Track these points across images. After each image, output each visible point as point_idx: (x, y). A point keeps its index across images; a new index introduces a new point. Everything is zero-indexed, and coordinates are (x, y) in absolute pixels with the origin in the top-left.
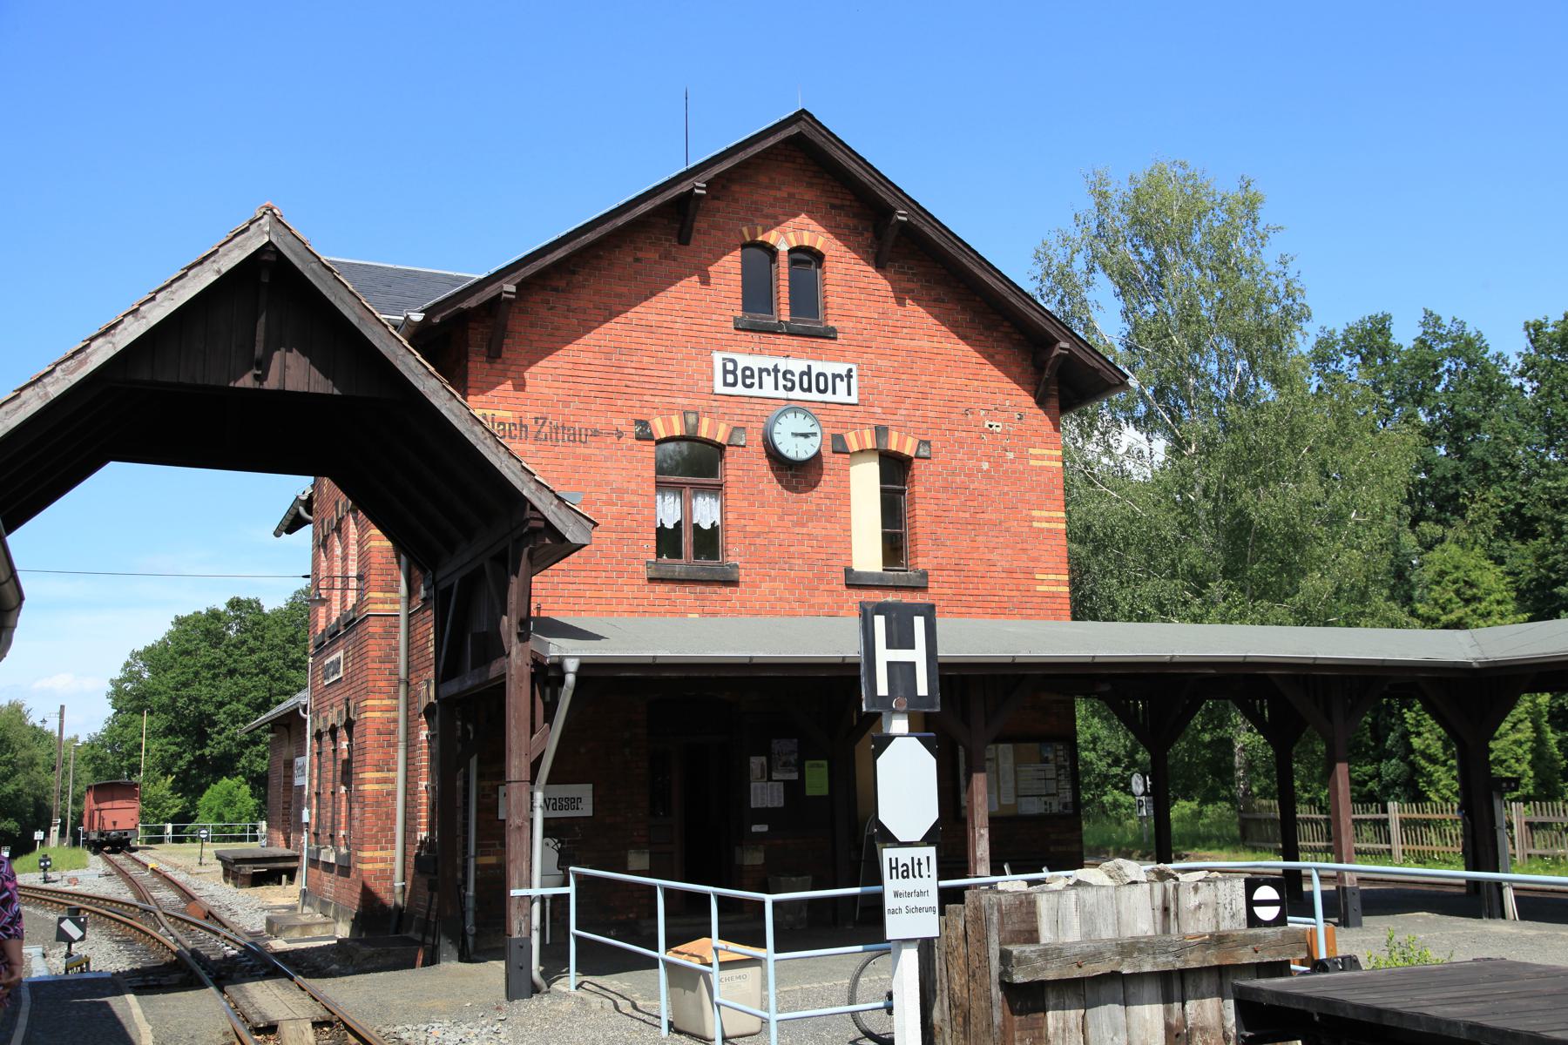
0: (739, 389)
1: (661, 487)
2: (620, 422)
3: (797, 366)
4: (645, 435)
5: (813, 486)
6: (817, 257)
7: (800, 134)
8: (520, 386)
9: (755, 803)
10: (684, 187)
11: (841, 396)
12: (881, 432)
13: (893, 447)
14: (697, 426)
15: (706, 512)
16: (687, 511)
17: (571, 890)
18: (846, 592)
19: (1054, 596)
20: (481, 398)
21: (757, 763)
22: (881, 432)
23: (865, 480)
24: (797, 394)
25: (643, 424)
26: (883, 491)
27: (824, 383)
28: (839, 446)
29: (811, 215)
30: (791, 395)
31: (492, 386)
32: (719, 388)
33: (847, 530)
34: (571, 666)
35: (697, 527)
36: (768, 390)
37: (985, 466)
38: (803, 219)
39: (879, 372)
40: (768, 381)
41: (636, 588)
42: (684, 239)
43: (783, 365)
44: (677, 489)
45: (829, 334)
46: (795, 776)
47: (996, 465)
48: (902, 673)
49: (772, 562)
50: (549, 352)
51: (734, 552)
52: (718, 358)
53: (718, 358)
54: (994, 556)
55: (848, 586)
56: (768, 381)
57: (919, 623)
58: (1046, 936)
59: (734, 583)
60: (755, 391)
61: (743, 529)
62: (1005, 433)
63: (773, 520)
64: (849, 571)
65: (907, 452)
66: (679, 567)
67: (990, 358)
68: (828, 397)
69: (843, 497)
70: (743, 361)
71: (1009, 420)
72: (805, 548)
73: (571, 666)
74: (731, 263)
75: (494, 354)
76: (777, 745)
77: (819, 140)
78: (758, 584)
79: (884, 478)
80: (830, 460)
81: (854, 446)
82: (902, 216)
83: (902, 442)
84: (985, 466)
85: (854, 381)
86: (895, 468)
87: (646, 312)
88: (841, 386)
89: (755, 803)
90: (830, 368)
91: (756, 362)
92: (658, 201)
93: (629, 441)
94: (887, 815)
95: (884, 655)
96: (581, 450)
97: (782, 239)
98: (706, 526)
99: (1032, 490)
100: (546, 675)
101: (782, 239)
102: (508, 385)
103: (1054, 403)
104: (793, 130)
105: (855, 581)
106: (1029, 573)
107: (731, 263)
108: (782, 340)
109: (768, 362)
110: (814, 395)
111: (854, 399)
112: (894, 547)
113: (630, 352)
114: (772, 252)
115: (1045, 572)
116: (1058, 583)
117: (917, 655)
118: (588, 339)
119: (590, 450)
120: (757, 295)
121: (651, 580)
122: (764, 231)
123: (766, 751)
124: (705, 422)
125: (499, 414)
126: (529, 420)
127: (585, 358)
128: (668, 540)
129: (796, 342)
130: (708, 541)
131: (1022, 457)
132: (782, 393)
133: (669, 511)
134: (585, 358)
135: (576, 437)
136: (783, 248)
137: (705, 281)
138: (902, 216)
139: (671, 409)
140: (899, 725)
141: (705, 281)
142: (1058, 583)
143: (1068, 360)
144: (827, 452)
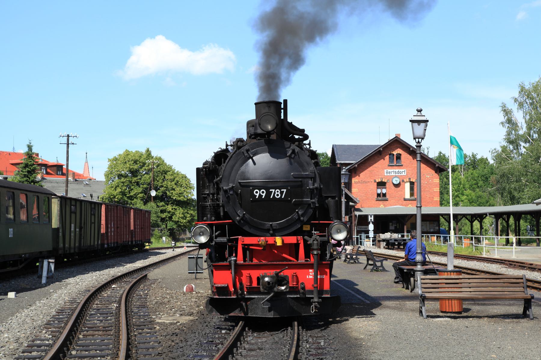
0: (388, 175)
1: (377, 188)
2: (372, 180)
3: (397, 170)
4: (375, 182)
5: (399, 187)
6: (400, 155)
7: (396, 139)
8: (359, 176)
9: (390, 229)
10: (379, 149)
11: (403, 174)
12: (410, 179)
13: (411, 181)
14: (382, 180)
15: (384, 191)
16: (382, 191)
17: (359, 236)
18: (404, 201)
19: (437, 201)
20: (354, 178)
21: (391, 224)
22: (410, 179)
23: (407, 186)
24: (397, 174)
25: (375, 180)
26: (410, 187)
27: (401, 173)
28: (403, 181)
29: (400, 148)
30: (396, 175)
31: (355, 177)
32: (386, 175)
33: (404, 193)
34: (357, 215)
35: (383, 193)
36: (393, 174)
37: (426, 182)
38: (399, 149)
39: (409, 170)
40: (393, 173)
41: (374, 202)
42: (381, 155)
43: (395, 170)
44: (380, 188)
45: (402, 166)
46: (396, 225)
47: (428, 182)
48: (371, 220)
49: (393, 197)
50: (362, 172)
51: (388, 197)
52: (385, 170)
53: (385, 170)
54: (427, 195)
55: (404, 200)
56: (393, 173)
57: (373, 216)
58: (381, 237)
59: (388, 200)
60: (391, 175)
61: (389, 193)
62: (430, 177)
63: (393, 192)
64: (404, 198)
65: (414, 181)
66: (380, 198)
67: (428, 166)
68: (402, 174)
69: (404, 188)
70: (389, 170)
71: (431, 175)
72: (398, 195)
73: (357, 215)
74: (387, 157)
75: (355, 173)
76: (393, 222)
77: (399, 140)
78: (391, 201)
79: (410, 185)
80: (401, 183)
81: (405, 181)
82: (411, 149)
83: (413, 180)
84: (426, 182)
85: (405, 172)
86: (412, 183)
87: (375, 165)
88: (403, 173)
89: (390, 229)
90: (402, 170)
91: (391, 170)
92: (376, 152)
93: (373, 183)
94: (369, 229)
95: (370, 218)
96: (367, 184)
97: (395, 153)
98: (384, 193)
99: (434, 185)
100: (356, 216)
101: (395, 153)
102: (358, 176)
103: (438, 172)
104: (395, 139)
105: (405, 200)
106: (433, 197)
107: (387, 157)
108: (395, 167)
109: (393, 170)
110: (399, 174)
111: (405, 174)
112: (412, 194)
113: (373, 171)
114: (393, 155)
115: (436, 197)
116: (438, 199)
117: (372, 218)
118: (368, 170)
119: (368, 184)
120: (391, 160)
121: (376, 201)
122: (393, 152)
123: (392, 222)
124: (384, 179)
125: (356, 180)
126: (360, 181)
127: (367, 172)
128: (379, 195)
129: (397, 167)
130: (384, 195)
131: (432, 181)
132: (395, 174)
133: (379, 191)
134: (367, 172)
135: (366, 183)
136: (395, 154)
137: (384, 160)
138: (411, 149)
139: (379, 178)
140: (371, 223)
141: (384, 160)
142: (438, 199)
143: (438, 167)
144: (401, 182)
